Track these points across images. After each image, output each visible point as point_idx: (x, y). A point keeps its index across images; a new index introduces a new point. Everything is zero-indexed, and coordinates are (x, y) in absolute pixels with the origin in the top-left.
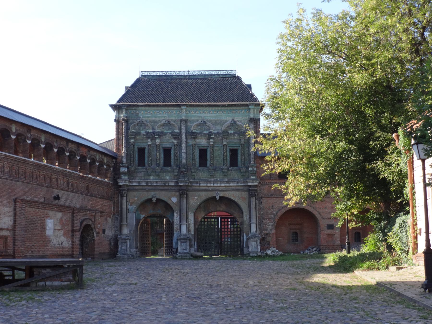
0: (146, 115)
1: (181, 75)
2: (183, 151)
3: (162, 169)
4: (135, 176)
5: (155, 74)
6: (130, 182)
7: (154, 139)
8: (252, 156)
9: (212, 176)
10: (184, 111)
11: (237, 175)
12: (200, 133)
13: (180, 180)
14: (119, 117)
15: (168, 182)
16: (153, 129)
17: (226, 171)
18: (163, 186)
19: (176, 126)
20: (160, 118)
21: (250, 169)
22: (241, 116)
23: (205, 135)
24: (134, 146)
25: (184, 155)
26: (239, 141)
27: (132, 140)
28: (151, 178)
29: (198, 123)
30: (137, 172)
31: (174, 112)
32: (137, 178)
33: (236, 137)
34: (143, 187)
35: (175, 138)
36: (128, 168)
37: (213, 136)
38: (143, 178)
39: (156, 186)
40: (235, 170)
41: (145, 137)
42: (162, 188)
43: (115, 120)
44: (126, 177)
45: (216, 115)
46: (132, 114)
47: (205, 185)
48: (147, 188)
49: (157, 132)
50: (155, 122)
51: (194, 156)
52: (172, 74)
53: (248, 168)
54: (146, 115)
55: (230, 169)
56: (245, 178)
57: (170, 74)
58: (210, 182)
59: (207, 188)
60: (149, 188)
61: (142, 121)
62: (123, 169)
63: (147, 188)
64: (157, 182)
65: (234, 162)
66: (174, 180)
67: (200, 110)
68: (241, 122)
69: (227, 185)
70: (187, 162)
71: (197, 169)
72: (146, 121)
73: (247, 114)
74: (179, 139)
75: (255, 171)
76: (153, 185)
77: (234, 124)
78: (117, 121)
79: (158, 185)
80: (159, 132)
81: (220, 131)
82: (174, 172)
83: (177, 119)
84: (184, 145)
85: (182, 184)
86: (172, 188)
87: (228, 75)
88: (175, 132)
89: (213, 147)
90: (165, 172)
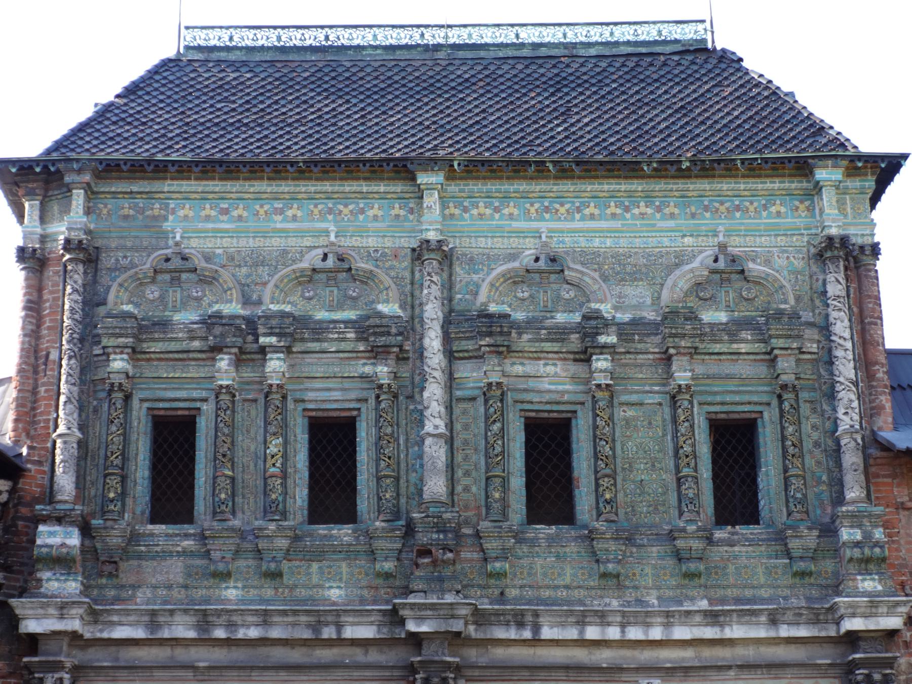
0: (206, 222)
1: (407, 47)
2: (429, 428)
3: (296, 538)
4: (126, 578)
5: (265, 39)
6: (94, 616)
7: (250, 356)
8: (851, 458)
9: (612, 580)
10: (431, 200)
11: (769, 571)
12: (531, 324)
13: (411, 600)
14: (43, 239)
15: (337, 616)
16: (246, 302)
17: (696, 544)
18: (304, 643)
19: (388, 281)
20: (292, 242)
21: (847, 534)
22: (766, 229)
23: (560, 334)
24: (128, 398)
25: (435, 452)
26: (762, 370)
27: (118, 363)
28: (232, 593)
29: (516, 264)
30: (140, 557)
31: (375, 211)
32: (142, 596)
33: (743, 348)
34: (182, 655)
35: (376, 353)
36: (86, 531)
37: (612, 339)
38: (176, 594)
39: (263, 641)
40: (752, 543)
41: (196, 344)
42: (296, 656)
43: (23, 254)
44: (73, 586)
45: (617, 224)
46: (126, 217)
47: (572, 633)
48: (203, 656)
49: (268, 317)
50: (257, 260)
51: (495, 458)
52: (358, 38)
53: (829, 531)
54: (210, 226)
55: (720, 534)
56: (815, 593)
57: (345, 38)
58: (602, 618)
59: (580, 655)
60: (219, 655)
61: (185, 259)
62: (54, 537)
63: (203, 656)
64: (265, 618)
65: (736, 499)
66: (375, 602)
67: (525, 196)
68: (768, 262)
69: (709, 633)
70: (452, 493)
71: (519, 538)
72: (208, 258)
73: (801, 219)
74: (402, 358)
75: (877, 544)
76: (241, 634)
77: (730, 271)
78: (33, 259)
79: (276, 633)
80: (283, 315)
81: (650, 315)
82: (372, 554)
83: (388, 243)
84: (434, 394)
85: (424, 628)
86: (359, 655)
87: (665, 42)
88: (380, 315)
89: (611, 404)
90: (318, 555)
